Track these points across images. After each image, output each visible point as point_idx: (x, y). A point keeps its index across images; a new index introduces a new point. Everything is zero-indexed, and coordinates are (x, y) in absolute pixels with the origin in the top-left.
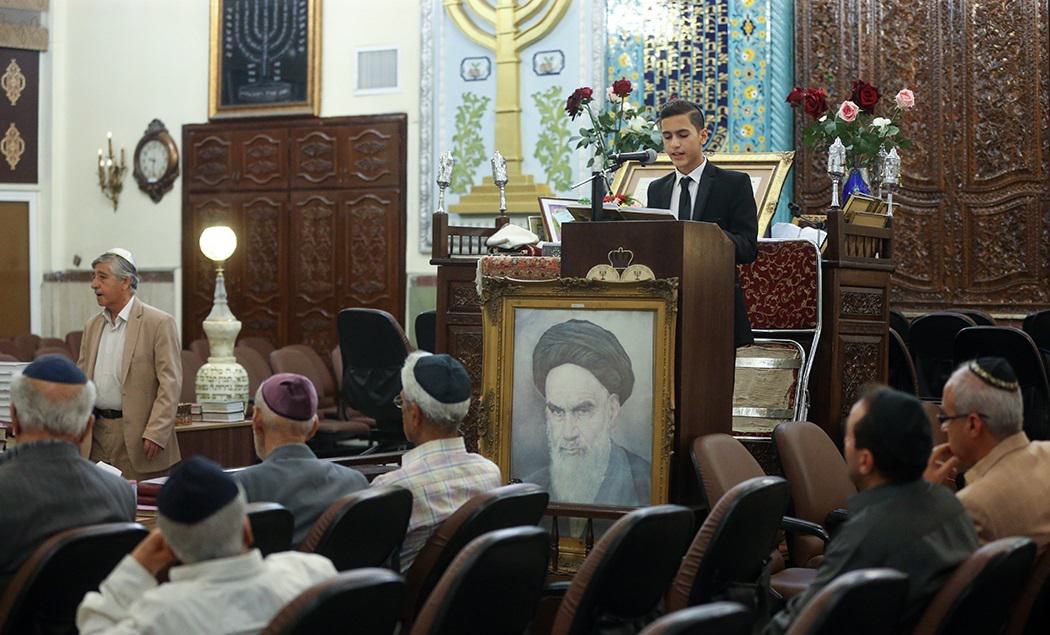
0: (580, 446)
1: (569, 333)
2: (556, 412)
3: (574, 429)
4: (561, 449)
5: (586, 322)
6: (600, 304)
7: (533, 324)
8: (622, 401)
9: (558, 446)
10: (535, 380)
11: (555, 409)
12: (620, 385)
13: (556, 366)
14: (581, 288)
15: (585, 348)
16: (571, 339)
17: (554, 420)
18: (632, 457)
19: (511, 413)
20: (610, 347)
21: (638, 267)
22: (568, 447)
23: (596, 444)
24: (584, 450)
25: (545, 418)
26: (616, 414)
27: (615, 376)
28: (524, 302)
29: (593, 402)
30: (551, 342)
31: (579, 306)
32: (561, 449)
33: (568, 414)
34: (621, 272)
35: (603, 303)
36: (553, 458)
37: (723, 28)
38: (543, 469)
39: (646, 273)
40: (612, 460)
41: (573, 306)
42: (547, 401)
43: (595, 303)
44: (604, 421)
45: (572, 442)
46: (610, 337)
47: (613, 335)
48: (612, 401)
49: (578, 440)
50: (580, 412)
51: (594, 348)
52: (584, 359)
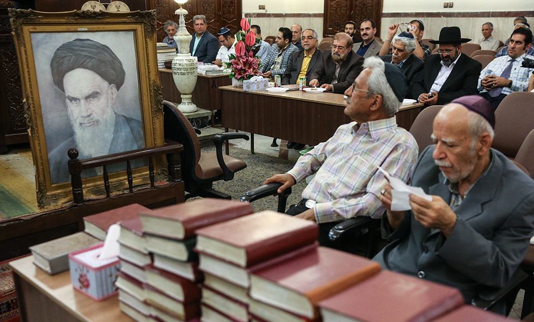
0: (94, 120)
1: (76, 48)
2: (73, 101)
3: (87, 111)
4: (81, 124)
5: (88, 40)
6: (98, 28)
8: (118, 88)
9: (78, 121)
11: (73, 99)
12: (115, 78)
13: (68, 71)
15: (90, 57)
16: (78, 52)
18: (128, 120)
19: (40, 107)
20: (106, 54)
22: (86, 122)
23: (105, 116)
24: (97, 121)
25: (66, 107)
26: (115, 96)
28: (39, 28)
29: (99, 91)
30: (63, 55)
31: (83, 29)
32: (81, 124)
33: (83, 101)
34: (106, 6)
35: (101, 27)
36: (75, 131)
38: (69, 139)
39: (124, 9)
41: (79, 29)
42: (67, 95)
43: (95, 27)
44: (108, 103)
45: (88, 118)
46: (105, 48)
47: (109, 49)
48: (112, 89)
49: (92, 116)
50: (91, 99)
51: (95, 57)
52: (90, 64)
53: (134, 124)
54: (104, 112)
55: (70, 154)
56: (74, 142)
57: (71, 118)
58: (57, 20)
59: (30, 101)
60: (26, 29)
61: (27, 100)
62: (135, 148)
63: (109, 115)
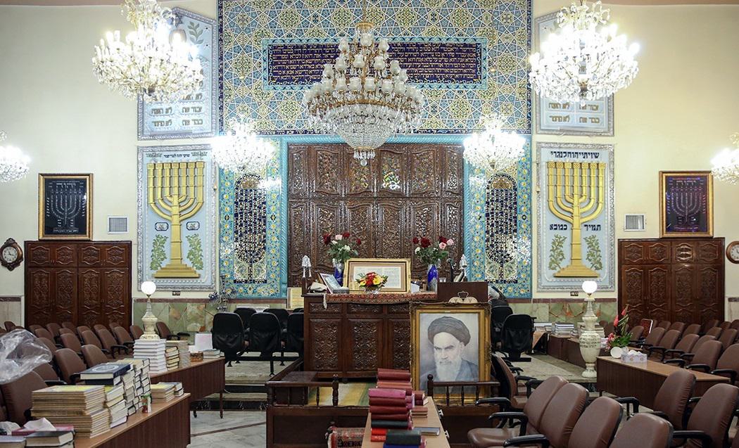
4: (441, 363)
7: (426, 319)
10: (429, 339)
11: (437, 348)
14: (447, 306)
17: (437, 352)
18: (470, 364)
21: (470, 298)
24: (451, 362)
27: (462, 335)
28: (424, 311)
32: (441, 363)
35: (458, 311)
37: (515, 217)
40: (462, 365)
53: (473, 367)
54: (455, 358)
55: (428, 377)
56: (435, 372)
57: (436, 358)
58: (434, 307)
59: (414, 347)
60: (418, 311)
61: (412, 346)
62: (472, 380)
63: (458, 360)
